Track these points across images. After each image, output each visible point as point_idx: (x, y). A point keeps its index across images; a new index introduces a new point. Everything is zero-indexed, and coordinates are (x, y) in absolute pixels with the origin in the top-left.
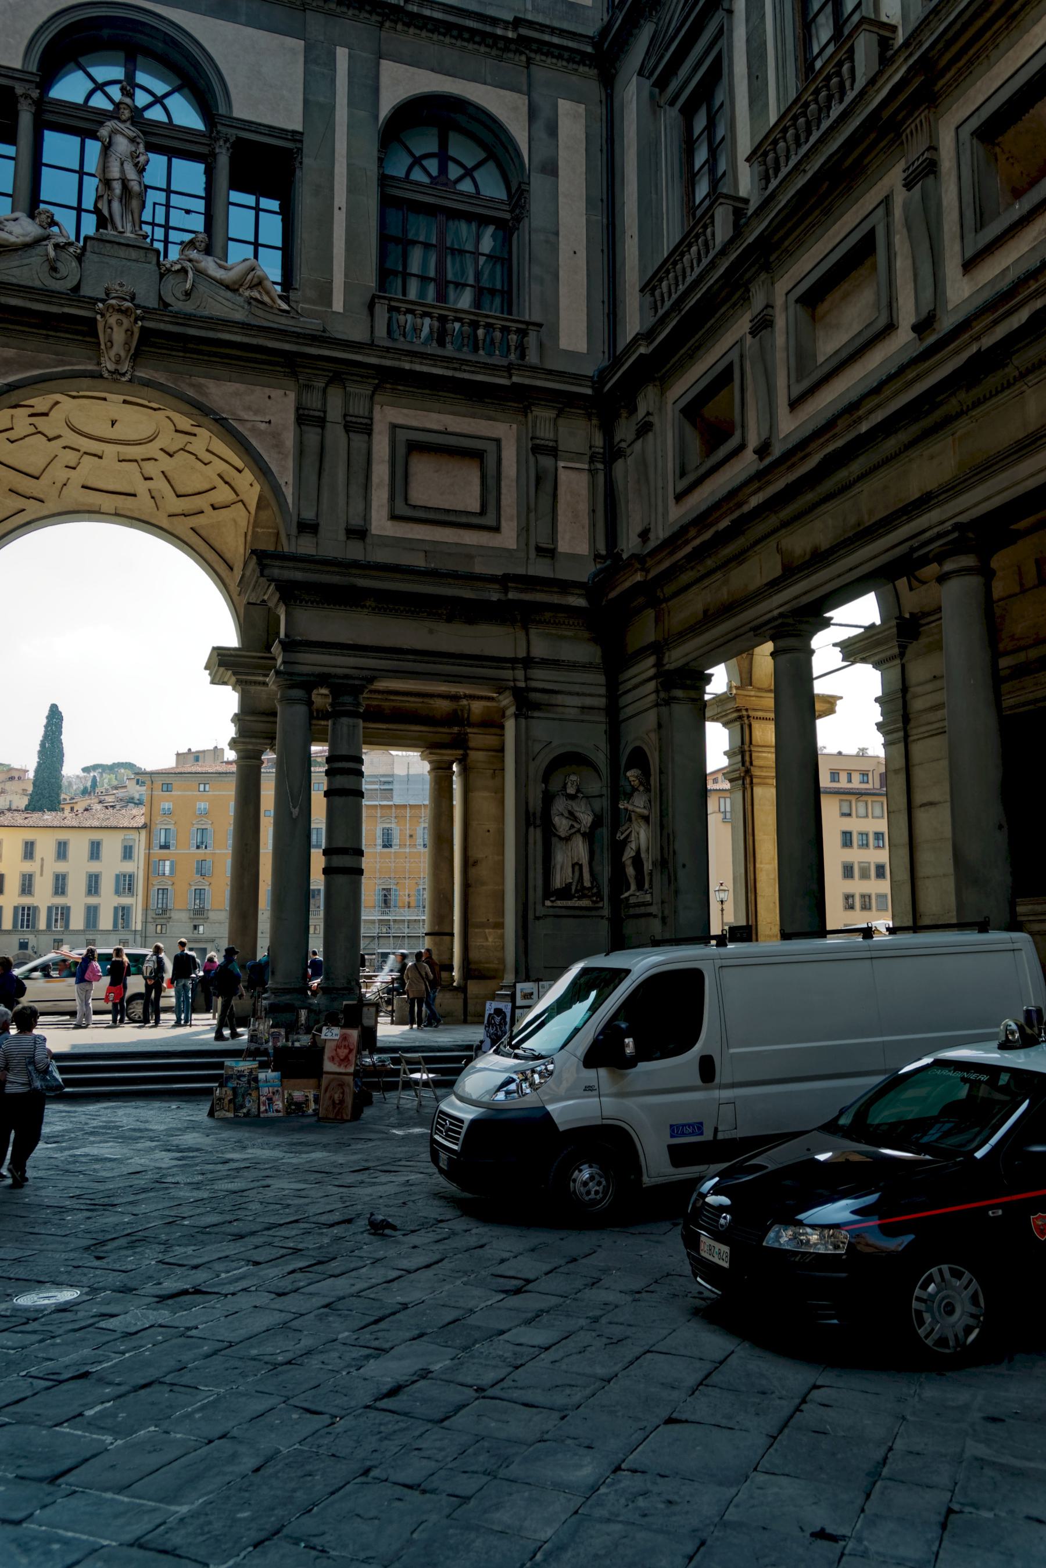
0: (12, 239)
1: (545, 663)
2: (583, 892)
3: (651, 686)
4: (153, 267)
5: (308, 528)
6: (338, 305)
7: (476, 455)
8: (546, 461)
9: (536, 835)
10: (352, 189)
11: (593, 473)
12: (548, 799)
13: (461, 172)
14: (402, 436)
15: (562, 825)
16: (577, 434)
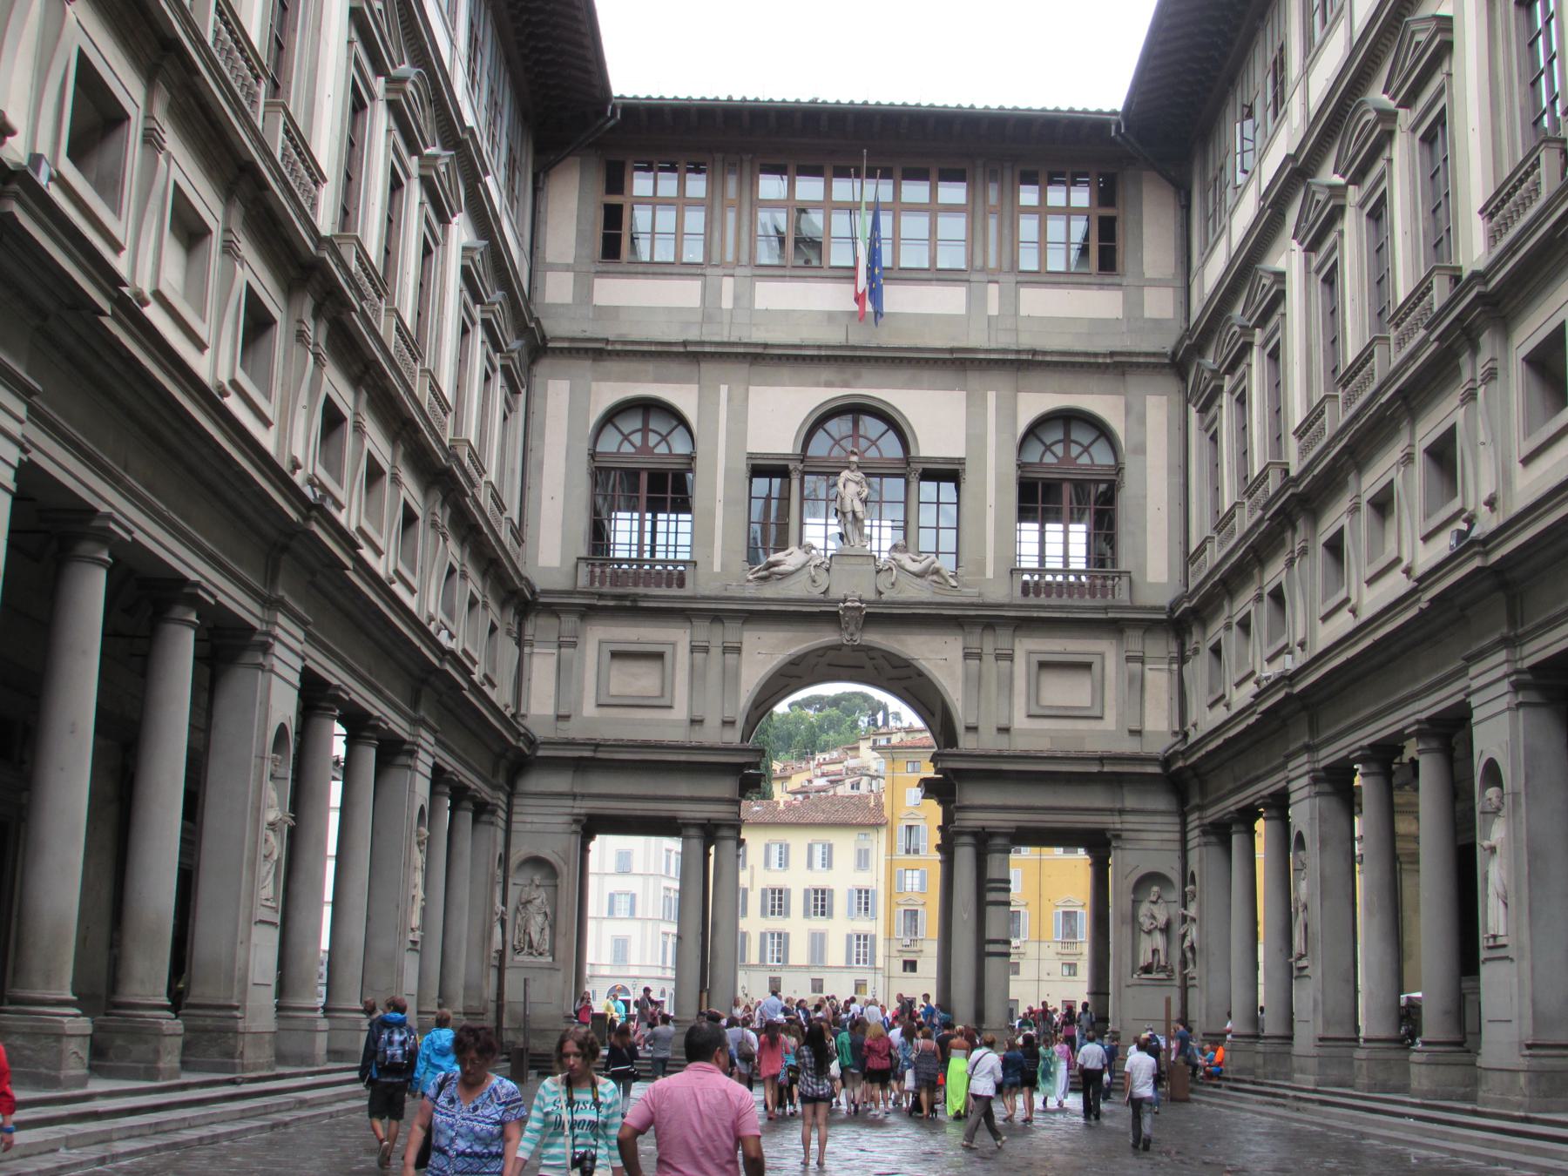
0: (791, 568)
1: (1134, 812)
2: (1164, 969)
3: (1196, 832)
4: (872, 567)
5: (972, 729)
6: (990, 574)
7: (1087, 666)
8: (1137, 666)
9: (1127, 930)
10: (998, 490)
11: (1170, 671)
12: (1136, 903)
13: (1079, 449)
14: (1035, 658)
15: (1147, 925)
16: (1160, 647)
